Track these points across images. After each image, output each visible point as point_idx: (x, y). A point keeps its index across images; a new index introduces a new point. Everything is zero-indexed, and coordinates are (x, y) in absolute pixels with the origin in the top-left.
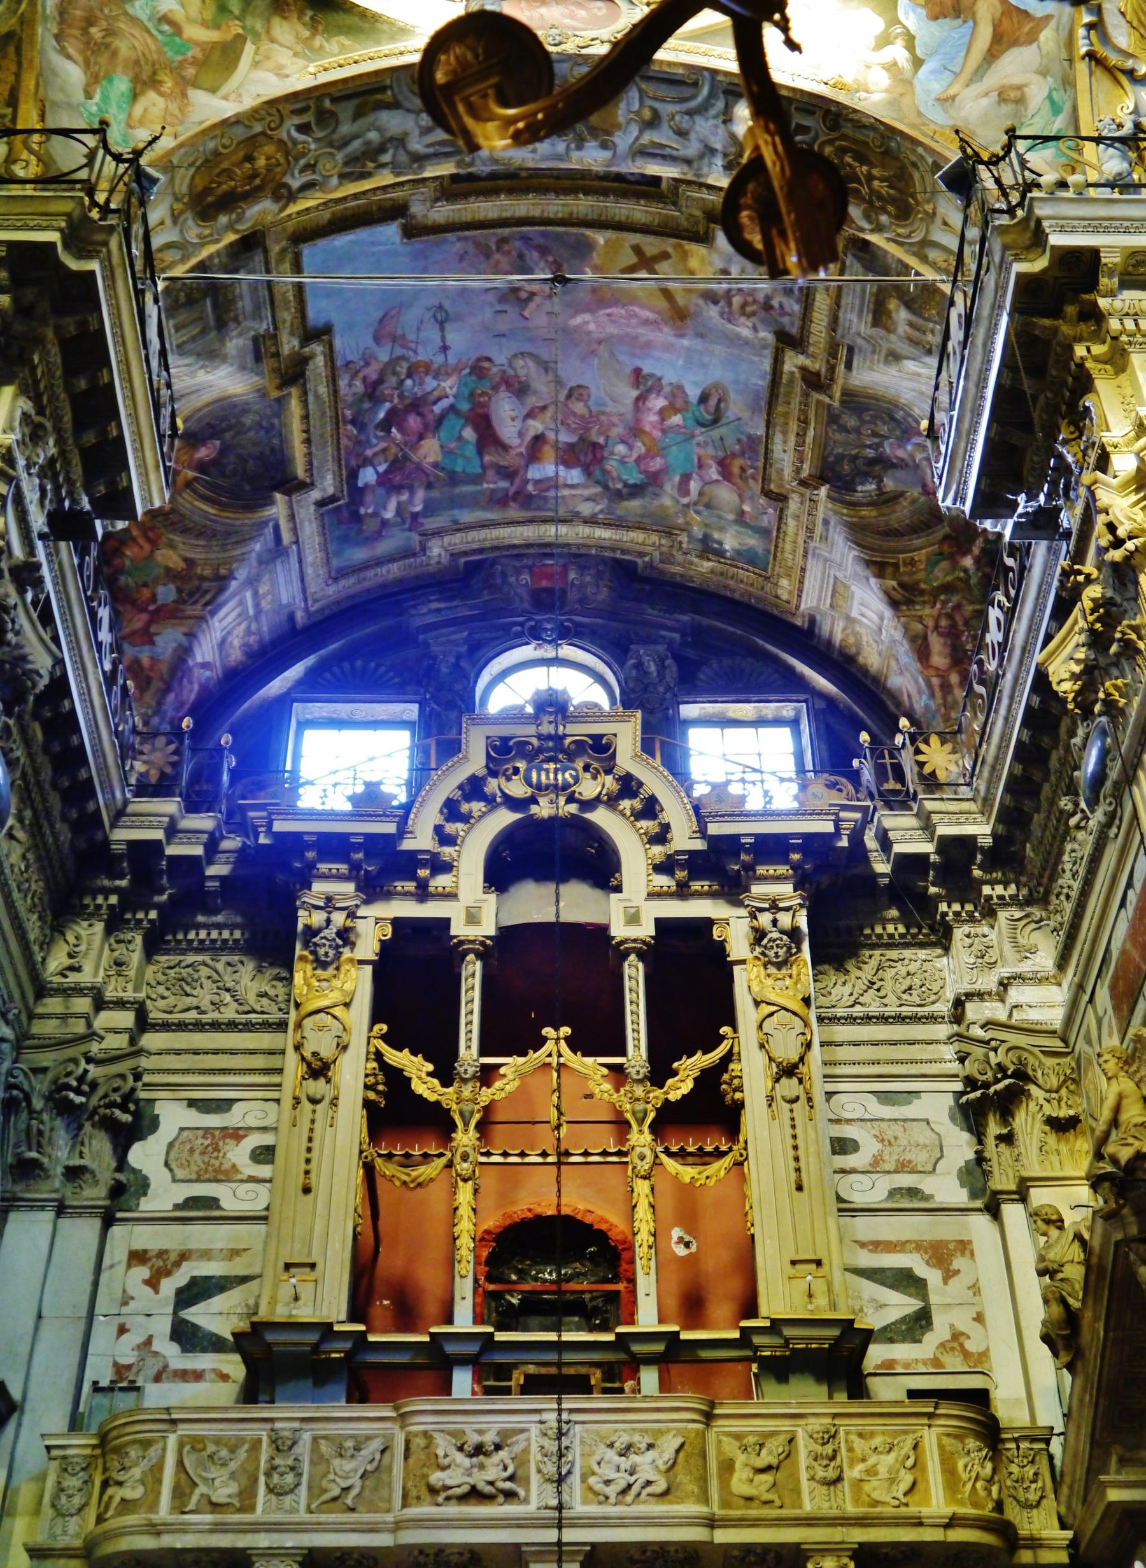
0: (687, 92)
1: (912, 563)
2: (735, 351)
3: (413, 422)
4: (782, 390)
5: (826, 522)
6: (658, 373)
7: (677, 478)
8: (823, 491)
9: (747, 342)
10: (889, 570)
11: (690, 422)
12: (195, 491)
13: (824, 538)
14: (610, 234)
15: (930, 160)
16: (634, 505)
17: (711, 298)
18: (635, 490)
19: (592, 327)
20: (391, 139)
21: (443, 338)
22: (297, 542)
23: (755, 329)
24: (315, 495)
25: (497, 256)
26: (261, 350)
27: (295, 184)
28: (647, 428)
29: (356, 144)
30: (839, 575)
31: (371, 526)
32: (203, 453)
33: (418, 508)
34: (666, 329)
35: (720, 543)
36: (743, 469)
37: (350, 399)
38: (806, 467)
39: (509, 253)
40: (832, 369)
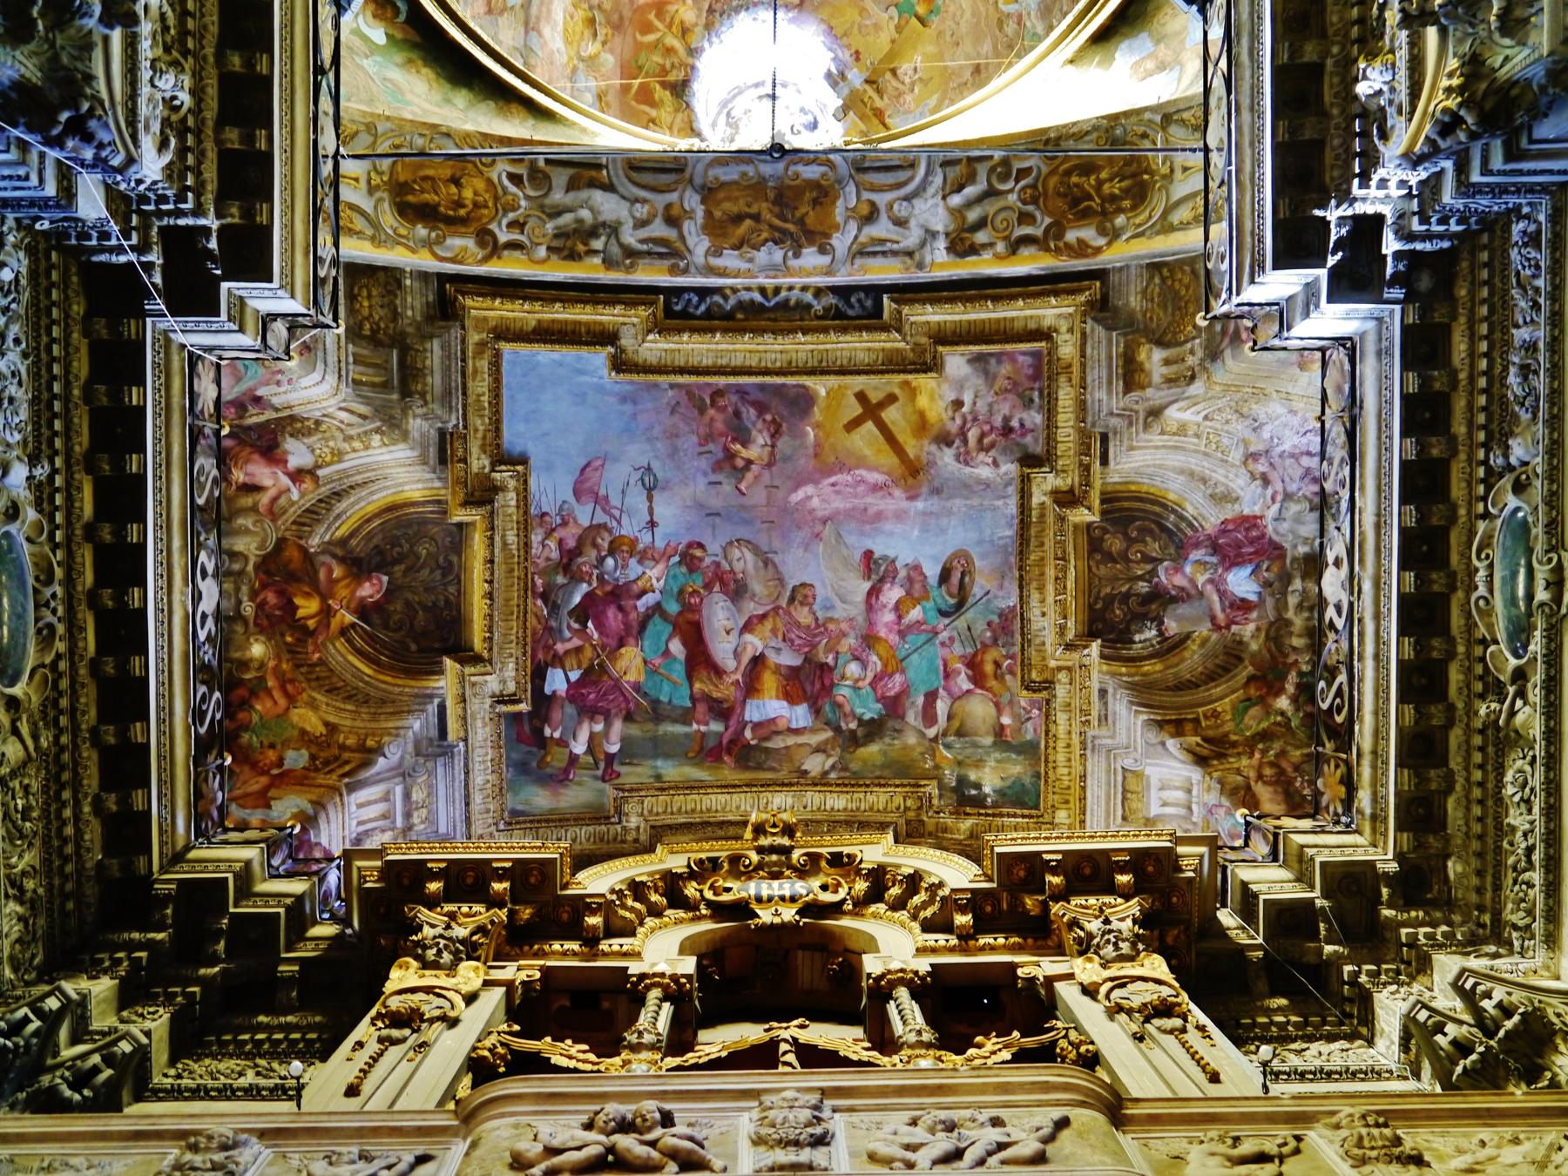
0: (902, 176)
1: (1215, 714)
2: (975, 502)
3: (612, 616)
4: (1033, 531)
5: (1103, 693)
6: (891, 553)
7: (920, 700)
8: (1095, 647)
9: (987, 485)
10: (1189, 727)
11: (933, 614)
12: (349, 641)
13: (1104, 719)
14: (833, 381)
15: (1158, 118)
16: (873, 750)
17: (944, 440)
18: (873, 729)
19: (815, 502)
20: (604, 224)
21: (651, 511)
22: (465, 740)
23: (996, 464)
24: (492, 684)
25: (712, 412)
26: (445, 450)
27: (503, 237)
28: (883, 633)
29: (567, 219)
30: (1128, 762)
31: (557, 759)
32: (367, 591)
33: (614, 749)
34: (897, 493)
35: (978, 786)
36: (997, 665)
37: (541, 563)
38: (1071, 624)
39: (723, 409)
40: (1086, 469)
